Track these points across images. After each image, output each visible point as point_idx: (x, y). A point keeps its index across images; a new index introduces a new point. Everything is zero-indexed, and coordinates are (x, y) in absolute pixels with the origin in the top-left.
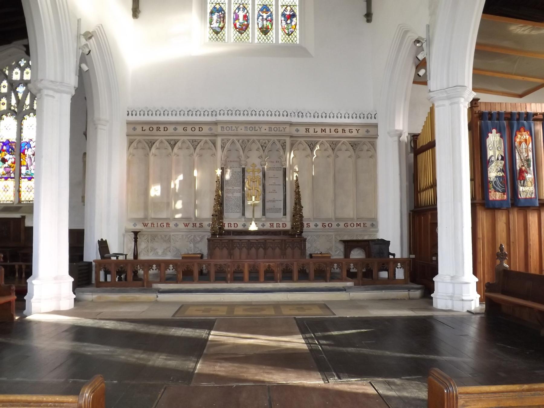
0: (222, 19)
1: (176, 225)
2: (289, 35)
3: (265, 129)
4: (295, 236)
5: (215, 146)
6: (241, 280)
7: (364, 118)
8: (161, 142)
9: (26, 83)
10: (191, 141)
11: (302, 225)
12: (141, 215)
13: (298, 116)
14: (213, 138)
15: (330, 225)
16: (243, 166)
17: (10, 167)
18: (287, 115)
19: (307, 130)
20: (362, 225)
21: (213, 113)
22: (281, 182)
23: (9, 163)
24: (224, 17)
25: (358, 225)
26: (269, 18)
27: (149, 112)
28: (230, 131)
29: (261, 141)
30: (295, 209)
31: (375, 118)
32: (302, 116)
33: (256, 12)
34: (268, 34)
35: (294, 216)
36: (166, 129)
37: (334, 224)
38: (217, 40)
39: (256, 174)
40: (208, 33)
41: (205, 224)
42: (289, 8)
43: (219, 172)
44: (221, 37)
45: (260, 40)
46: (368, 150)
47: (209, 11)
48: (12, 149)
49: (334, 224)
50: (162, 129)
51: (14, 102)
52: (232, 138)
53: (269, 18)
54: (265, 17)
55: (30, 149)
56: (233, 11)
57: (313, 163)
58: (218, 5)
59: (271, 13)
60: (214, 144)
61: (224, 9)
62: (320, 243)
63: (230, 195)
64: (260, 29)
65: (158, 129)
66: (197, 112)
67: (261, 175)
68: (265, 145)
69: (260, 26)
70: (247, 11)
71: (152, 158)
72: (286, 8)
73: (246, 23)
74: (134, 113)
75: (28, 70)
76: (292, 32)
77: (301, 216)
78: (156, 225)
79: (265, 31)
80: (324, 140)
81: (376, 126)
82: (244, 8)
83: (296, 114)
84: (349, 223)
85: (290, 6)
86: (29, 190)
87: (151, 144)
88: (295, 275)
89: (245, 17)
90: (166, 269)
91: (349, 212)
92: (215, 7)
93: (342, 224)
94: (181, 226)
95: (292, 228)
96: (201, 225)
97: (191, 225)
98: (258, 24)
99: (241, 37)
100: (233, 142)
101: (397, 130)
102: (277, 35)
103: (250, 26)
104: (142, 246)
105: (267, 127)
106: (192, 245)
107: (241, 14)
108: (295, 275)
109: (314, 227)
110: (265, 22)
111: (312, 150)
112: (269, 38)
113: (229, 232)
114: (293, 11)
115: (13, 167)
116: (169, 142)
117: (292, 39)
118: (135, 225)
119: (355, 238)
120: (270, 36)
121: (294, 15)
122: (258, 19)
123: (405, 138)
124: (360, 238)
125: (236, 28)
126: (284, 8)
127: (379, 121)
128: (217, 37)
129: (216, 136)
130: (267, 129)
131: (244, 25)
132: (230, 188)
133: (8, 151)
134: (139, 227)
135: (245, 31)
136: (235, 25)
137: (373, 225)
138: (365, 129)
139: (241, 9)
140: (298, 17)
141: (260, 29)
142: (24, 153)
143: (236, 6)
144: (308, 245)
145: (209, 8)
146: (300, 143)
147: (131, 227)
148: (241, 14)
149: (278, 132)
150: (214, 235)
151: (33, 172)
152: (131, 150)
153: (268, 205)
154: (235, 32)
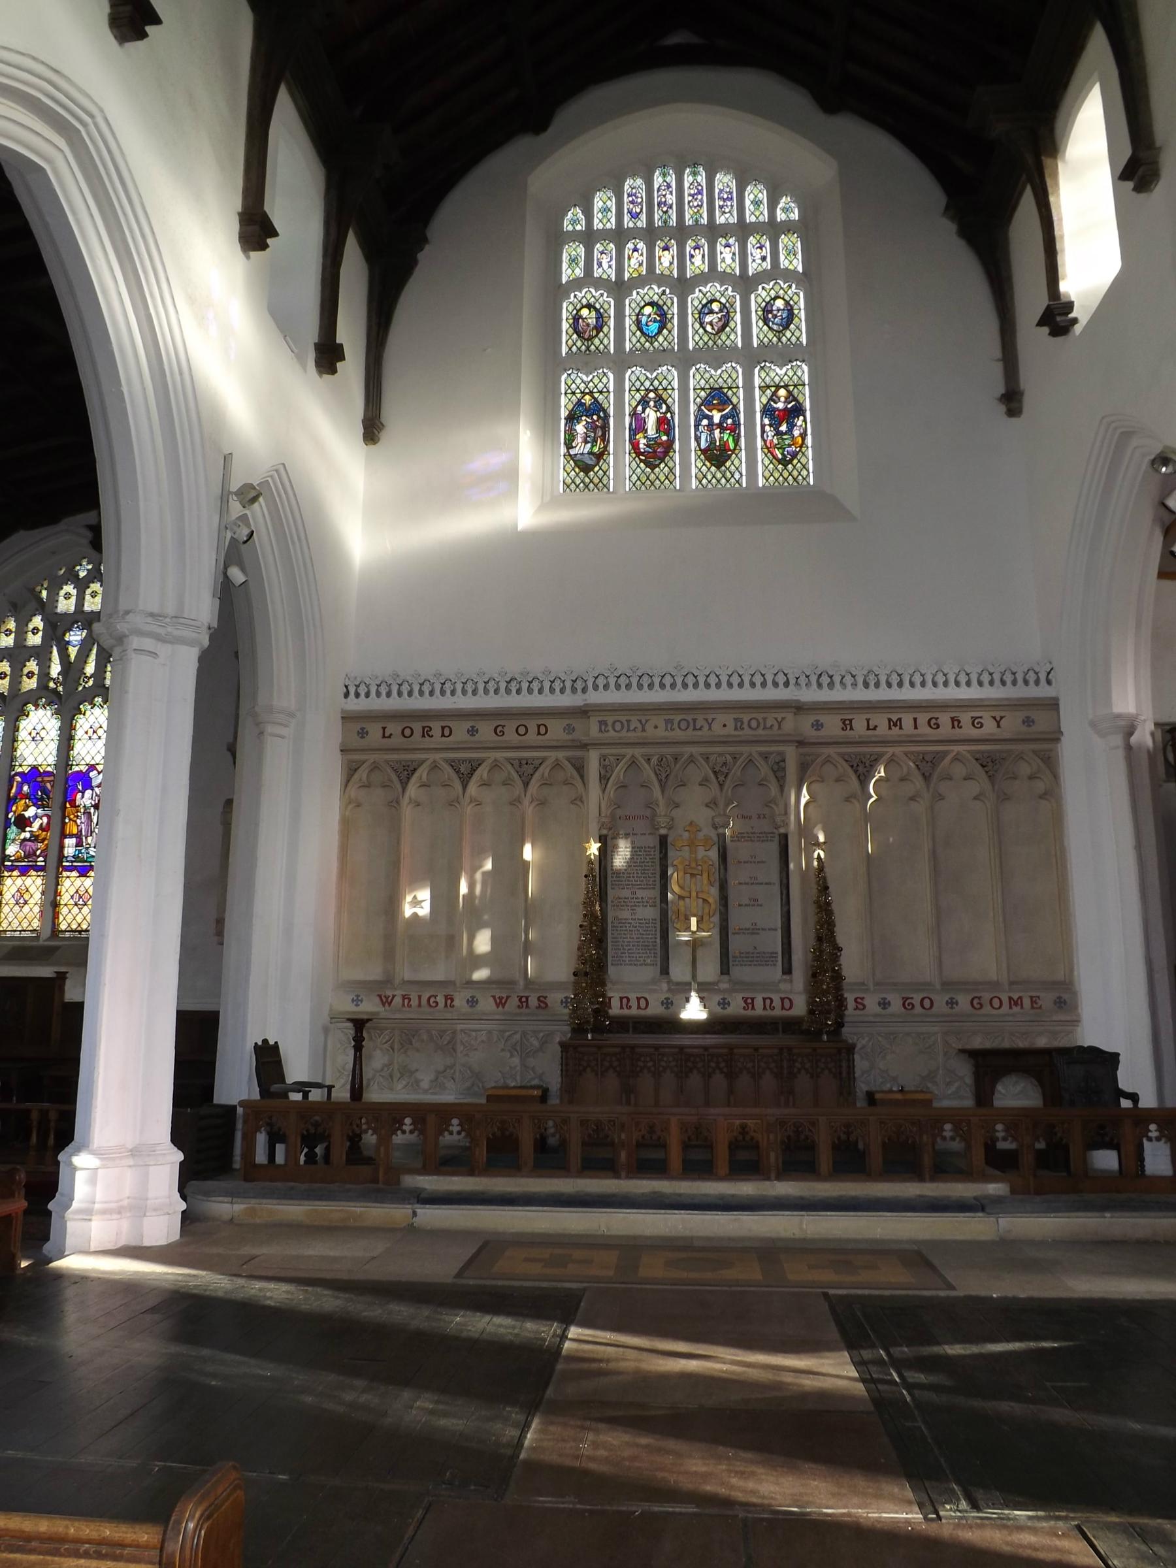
1: (472, 1002)
2: (784, 462)
3: (723, 726)
4: (815, 1038)
5: (582, 777)
6: (658, 1169)
7: (1014, 683)
8: (435, 767)
9: (85, 620)
10: (516, 763)
11: (841, 1002)
12: (374, 972)
13: (820, 685)
14: (578, 753)
15: (928, 1004)
16: (663, 832)
17: (34, 838)
18: (787, 684)
19: (847, 724)
20: (1027, 1002)
21: (578, 684)
22: (775, 877)
23: (36, 826)
24: (605, 428)
25: (1015, 1002)
26: (730, 421)
27: (402, 687)
28: (624, 733)
29: (712, 758)
30: (818, 955)
31: (1049, 682)
32: (831, 685)
33: (693, 408)
34: (728, 464)
35: (814, 975)
36: (447, 732)
37: (940, 1000)
38: (587, 486)
39: (701, 853)
40: (562, 471)
41: (555, 998)
42: (782, 392)
43: (594, 848)
44: (596, 480)
45: (704, 481)
46: (1031, 778)
47: (564, 413)
48: (45, 791)
49: (940, 1000)
50: (436, 732)
51: (55, 669)
52: (629, 752)
53: (730, 421)
54: (717, 420)
55: (88, 793)
56: (627, 410)
57: (867, 817)
58: (587, 397)
59: (735, 407)
60: (580, 768)
61: (605, 406)
62: (899, 1058)
63: (626, 914)
64: (704, 452)
65: (426, 732)
66: (533, 684)
67: (714, 854)
68: (724, 769)
69: (703, 445)
71: (407, 812)
73: (664, 438)
74: (362, 690)
75: (96, 586)
76: (794, 455)
77: (838, 977)
78: (414, 1002)
79: (717, 456)
80: (898, 750)
81: (1053, 705)
82: (660, 400)
83: (814, 679)
84: (986, 996)
85: (786, 387)
86: (80, 900)
87: (406, 772)
88: (825, 1158)
89: (664, 424)
90: (441, 1133)
91: (985, 962)
92: (579, 403)
93: (963, 1001)
94: (486, 1004)
95: (811, 1012)
96: (543, 1003)
97: (514, 1001)
98: (698, 439)
99: (652, 477)
100: (633, 763)
101: (1119, 716)
102: (754, 467)
103: (677, 446)
104: (376, 1061)
105: (728, 718)
106: (516, 1061)
107: (651, 417)
108: (825, 1158)
109: (878, 1010)
110: (717, 432)
111: (863, 781)
112: (728, 475)
113: (623, 1024)
114: (795, 399)
115: (43, 841)
116: (453, 764)
117: (795, 473)
118: (357, 1001)
119: (1006, 1044)
120: (733, 468)
121: (798, 410)
122: (697, 426)
123: (1145, 736)
124: (1022, 1044)
126: (768, 392)
127: (1064, 690)
128: (587, 480)
129: (584, 746)
130: (731, 725)
131: (662, 444)
132: (626, 893)
134: (370, 1006)
135: (663, 460)
137: (1060, 1003)
138: (1021, 715)
139: (652, 404)
140: (808, 414)
141: (704, 452)
142: (73, 805)
143: (638, 397)
144: (860, 1064)
145: (565, 405)
146: (828, 760)
147: (346, 1006)
148: (651, 417)
149: (760, 732)
150: (579, 1030)
151: (92, 852)
152: (353, 791)
153: (737, 944)
154: (634, 465)
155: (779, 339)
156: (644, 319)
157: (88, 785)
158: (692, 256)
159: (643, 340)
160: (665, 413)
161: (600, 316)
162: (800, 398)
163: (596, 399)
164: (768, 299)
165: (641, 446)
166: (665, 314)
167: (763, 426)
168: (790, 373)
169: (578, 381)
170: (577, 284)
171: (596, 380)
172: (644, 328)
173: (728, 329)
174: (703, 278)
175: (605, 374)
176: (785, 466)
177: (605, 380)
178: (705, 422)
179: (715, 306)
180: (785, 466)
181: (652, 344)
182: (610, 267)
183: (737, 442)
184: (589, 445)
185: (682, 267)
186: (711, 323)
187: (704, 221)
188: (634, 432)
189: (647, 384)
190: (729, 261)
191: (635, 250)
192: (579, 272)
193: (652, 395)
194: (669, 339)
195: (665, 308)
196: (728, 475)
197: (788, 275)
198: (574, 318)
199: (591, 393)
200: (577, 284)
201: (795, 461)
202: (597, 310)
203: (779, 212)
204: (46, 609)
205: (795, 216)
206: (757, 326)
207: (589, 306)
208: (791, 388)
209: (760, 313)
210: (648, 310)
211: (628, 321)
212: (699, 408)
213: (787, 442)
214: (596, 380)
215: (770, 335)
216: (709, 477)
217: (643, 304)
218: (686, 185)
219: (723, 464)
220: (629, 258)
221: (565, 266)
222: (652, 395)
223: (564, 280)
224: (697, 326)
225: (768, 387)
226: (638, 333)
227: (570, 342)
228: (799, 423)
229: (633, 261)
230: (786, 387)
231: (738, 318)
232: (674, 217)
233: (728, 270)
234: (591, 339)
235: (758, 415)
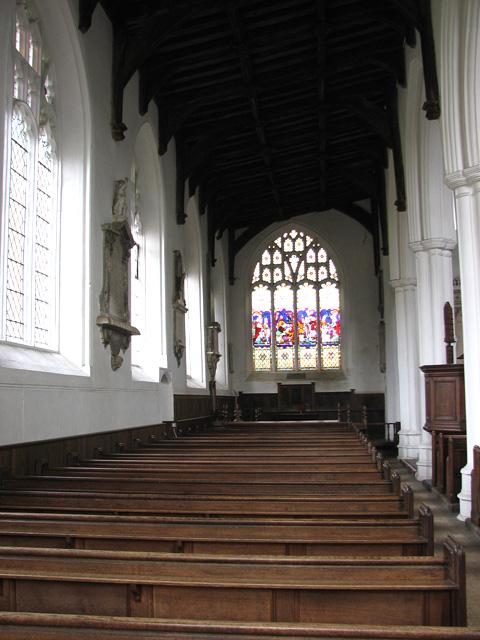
9: (297, 254)
23: (287, 331)
75: (299, 241)
133: (284, 320)
157: (304, 313)
204: (281, 250)
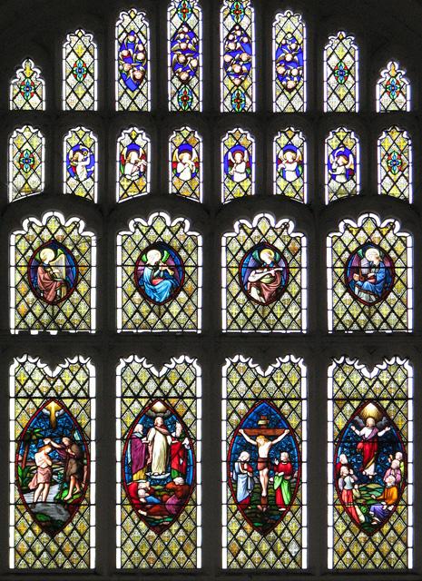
0: (73, 468)
2: (369, 528)
24: (83, 457)
26: (284, 456)
34: (280, 528)
45: (241, 556)
53: (284, 456)
54: (263, 452)
58: (53, 405)
61: (83, 421)
64: (242, 506)
69: (241, 494)
70: (186, 429)
72: (358, 411)
73: (179, 480)
76: (386, 516)
79: (263, 514)
82: (172, 416)
89: (176, 453)
92: (40, 415)
99: (158, 546)
103: (199, 494)
112: (280, 547)
114: (391, 423)
117: (385, 547)
121: (393, 442)
122: (231, 462)
125: (136, 505)
128: (53, 547)
135: (175, 518)
136: (131, 494)
139: (159, 421)
140: (410, 447)
141: (242, 506)
143: (136, 408)
154: (129, 524)
155: (369, 318)
156: (147, 272)
158: (230, 164)
159: (145, 308)
160: (180, 439)
161: (73, 264)
162: (399, 422)
163: (67, 409)
164: (353, 247)
165: (141, 492)
166: (183, 265)
167: (337, 466)
168: (385, 378)
169: (37, 376)
170: (34, 205)
171: (67, 377)
172: (148, 288)
173: (286, 296)
174: (246, 206)
175: (81, 365)
176: (370, 535)
177: (81, 377)
178: (245, 456)
179: (266, 256)
180: (370, 535)
181: (160, 316)
182: (89, 175)
183: (294, 491)
184: (56, 489)
185: (212, 183)
186: (258, 284)
187: (250, 105)
188: (129, 469)
189: (151, 386)
190: (291, 176)
191: (133, 147)
192: (37, 181)
193: (159, 406)
194: (186, 313)
195: (182, 254)
196: (280, 547)
197: (388, 206)
198: (29, 265)
199: (58, 399)
200: (34, 205)
201: (386, 528)
202: (68, 253)
203: (379, 90)
205: (404, 102)
206: (335, 296)
207: (54, 244)
208: (385, 403)
209: (340, 271)
210: (154, 256)
211: (120, 276)
212: (236, 432)
213: (375, 494)
214: (67, 377)
215: (355, 310)
216: (249, 550)
217: (144, 244)
218: (223, 33)
219: (272, 527)
220: (123, 163)
221: (12, 170)
222: (159, 406)
223: (12, 196)
224: (235, 288)
225: (348, 400)
226: (137, 297)
227: (23, 307)
228: (395, 463)
229: (129, 168)
230: (376, 401)
231: (303, 278)
232: (200, 91)
233: (290, 193)
234: (57, 302)
235: (330, 447)
